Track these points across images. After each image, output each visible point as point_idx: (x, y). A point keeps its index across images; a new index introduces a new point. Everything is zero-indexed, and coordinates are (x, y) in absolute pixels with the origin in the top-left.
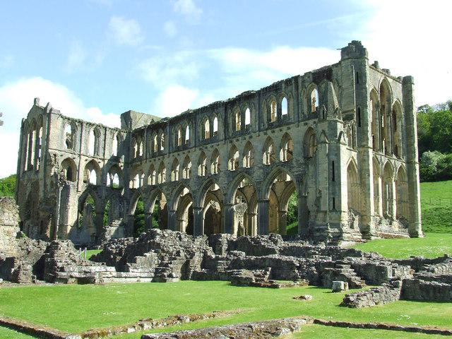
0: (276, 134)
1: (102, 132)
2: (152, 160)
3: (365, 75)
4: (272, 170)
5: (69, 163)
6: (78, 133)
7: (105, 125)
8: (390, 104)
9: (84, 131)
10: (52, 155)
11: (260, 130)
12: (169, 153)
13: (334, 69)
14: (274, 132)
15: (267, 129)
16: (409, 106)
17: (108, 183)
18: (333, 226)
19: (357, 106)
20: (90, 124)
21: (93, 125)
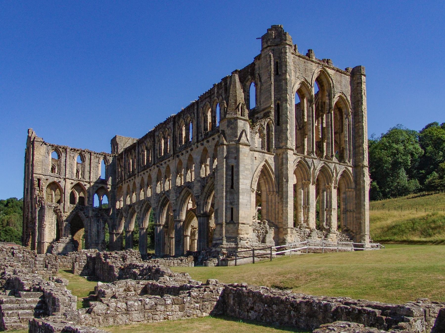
0: (210, 144)
1: (87, 156)
2: (128, 180)
3: (286, 64)
4: (207, 183)
5: (54, 186)
6: (63, 159)
7: (90, 150)
8: (330, 99)
9: (68, 156)
10: (35, 179)
11: (198, 142)
12: (138, 173)
13: (257, 63)
14: (208, 142)
15: (203, 140)
16: (359, 101)
17: (96, 204)
18: (229, 239)
19: (275, 101)
20: (75, 150)
21: (78, 150)
